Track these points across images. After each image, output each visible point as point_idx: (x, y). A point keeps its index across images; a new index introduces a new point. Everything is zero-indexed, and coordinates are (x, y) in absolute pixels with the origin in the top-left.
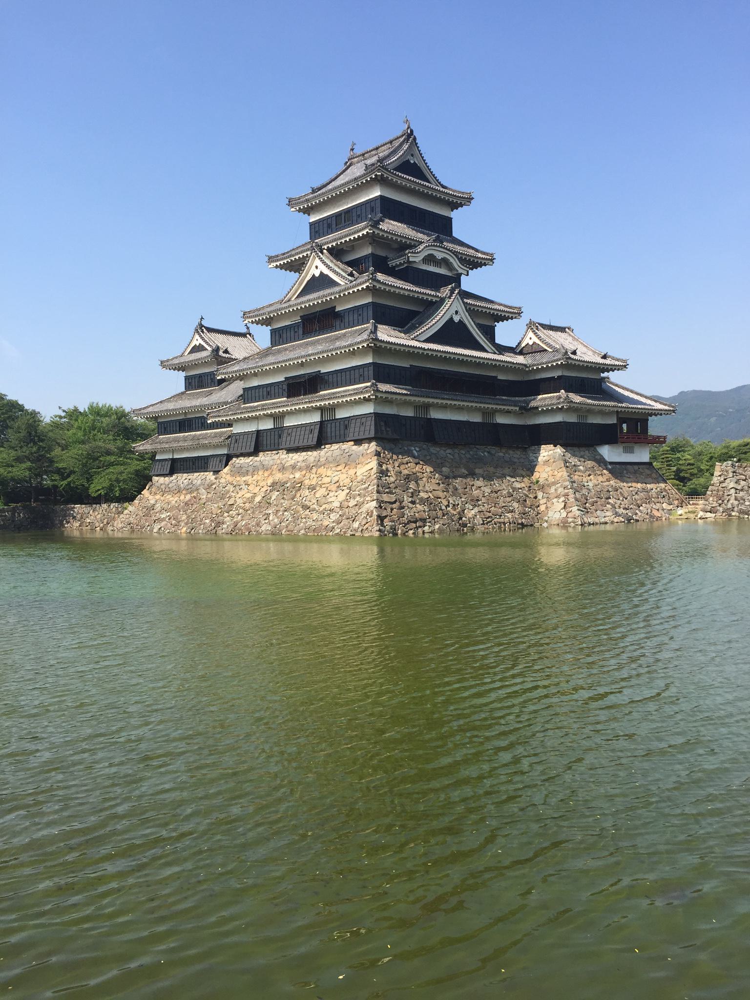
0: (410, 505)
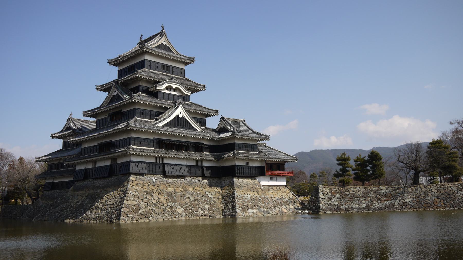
0: (144, 207)
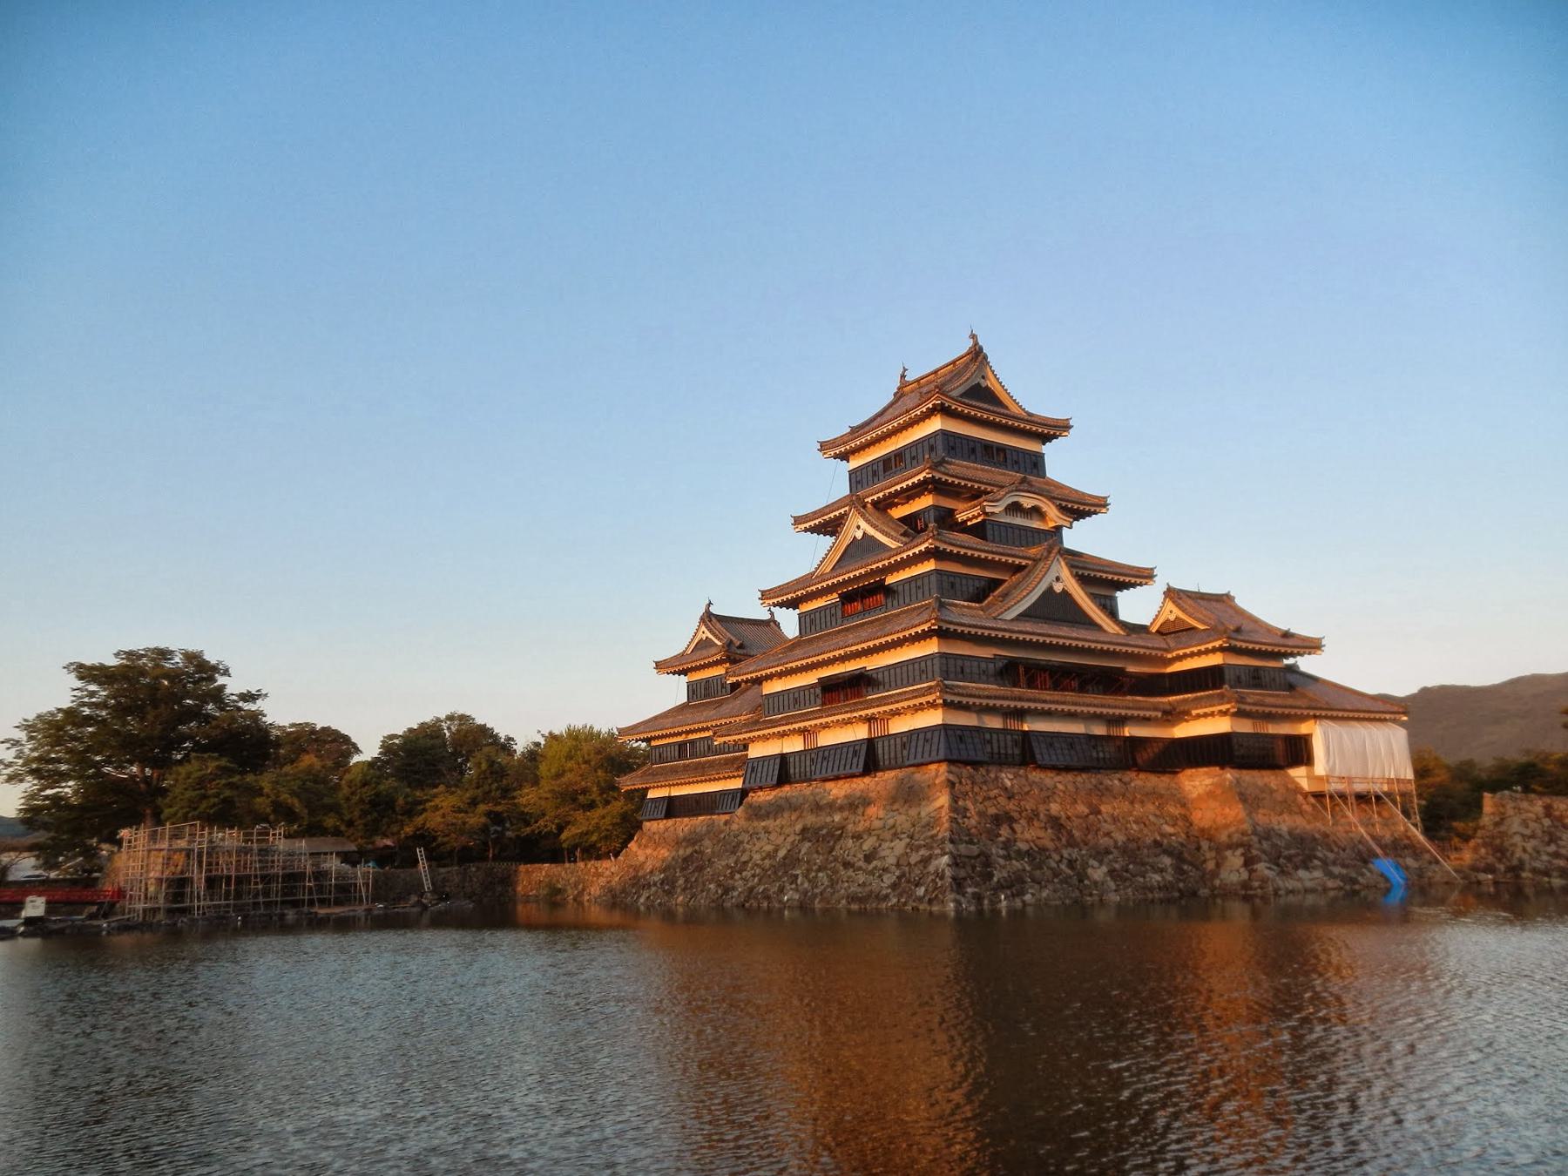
0: (1002, 861)
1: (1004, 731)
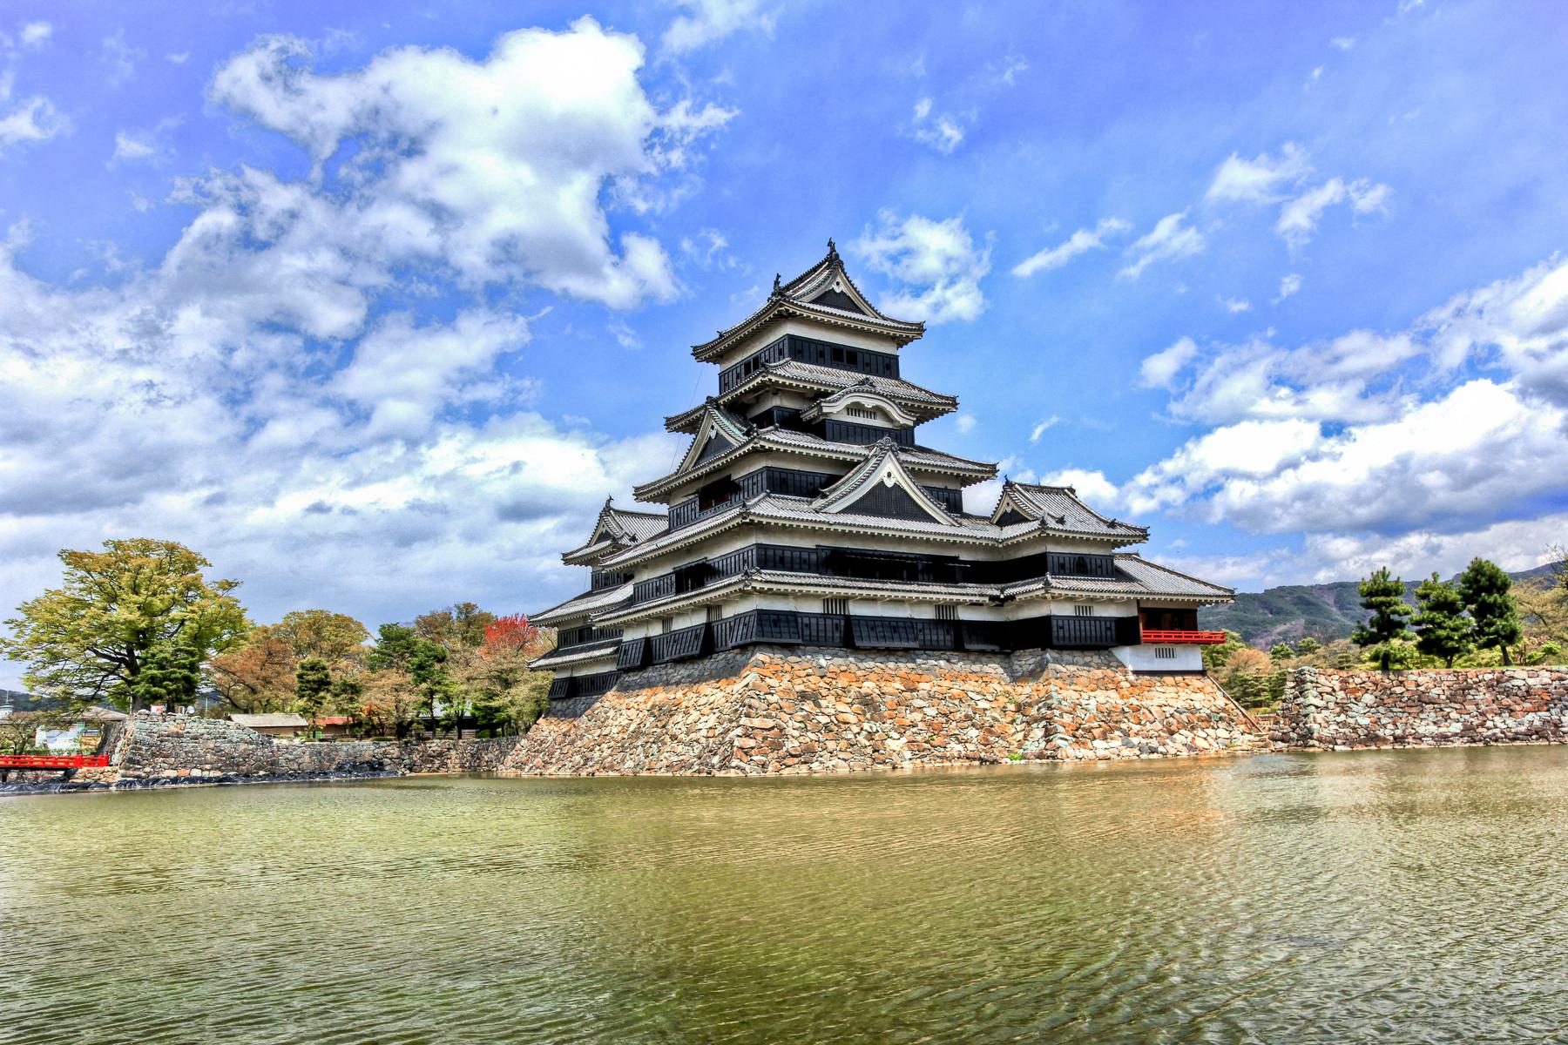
0: (796, 733)
1: (824, 616)
